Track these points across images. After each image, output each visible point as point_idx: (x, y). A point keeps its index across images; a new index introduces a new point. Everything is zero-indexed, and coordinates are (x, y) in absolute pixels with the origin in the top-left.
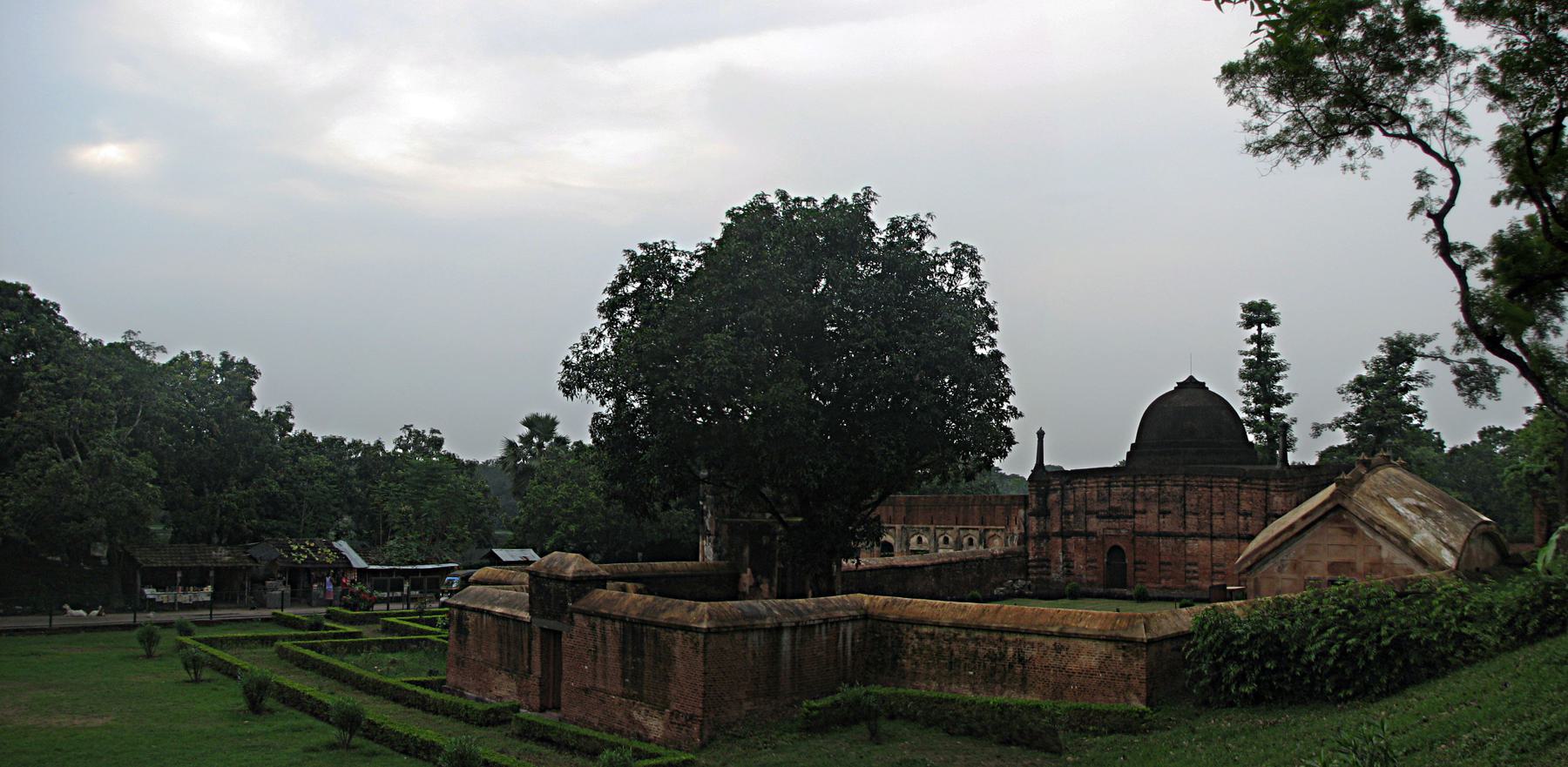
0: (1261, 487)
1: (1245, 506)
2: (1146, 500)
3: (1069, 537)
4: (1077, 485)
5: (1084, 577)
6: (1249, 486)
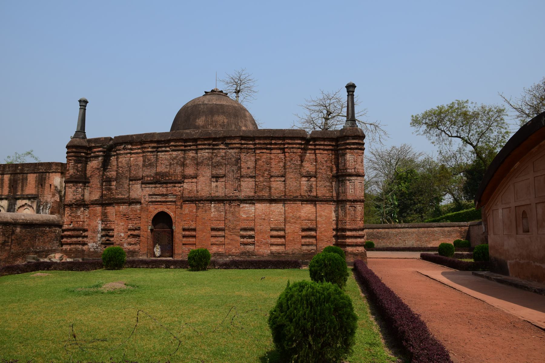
0: (326, 148)
1: (308, 167)
2: (197, 164)
3: (110, 204)
4: (122, 152)
5: (125, 246)
6: (313, 147)
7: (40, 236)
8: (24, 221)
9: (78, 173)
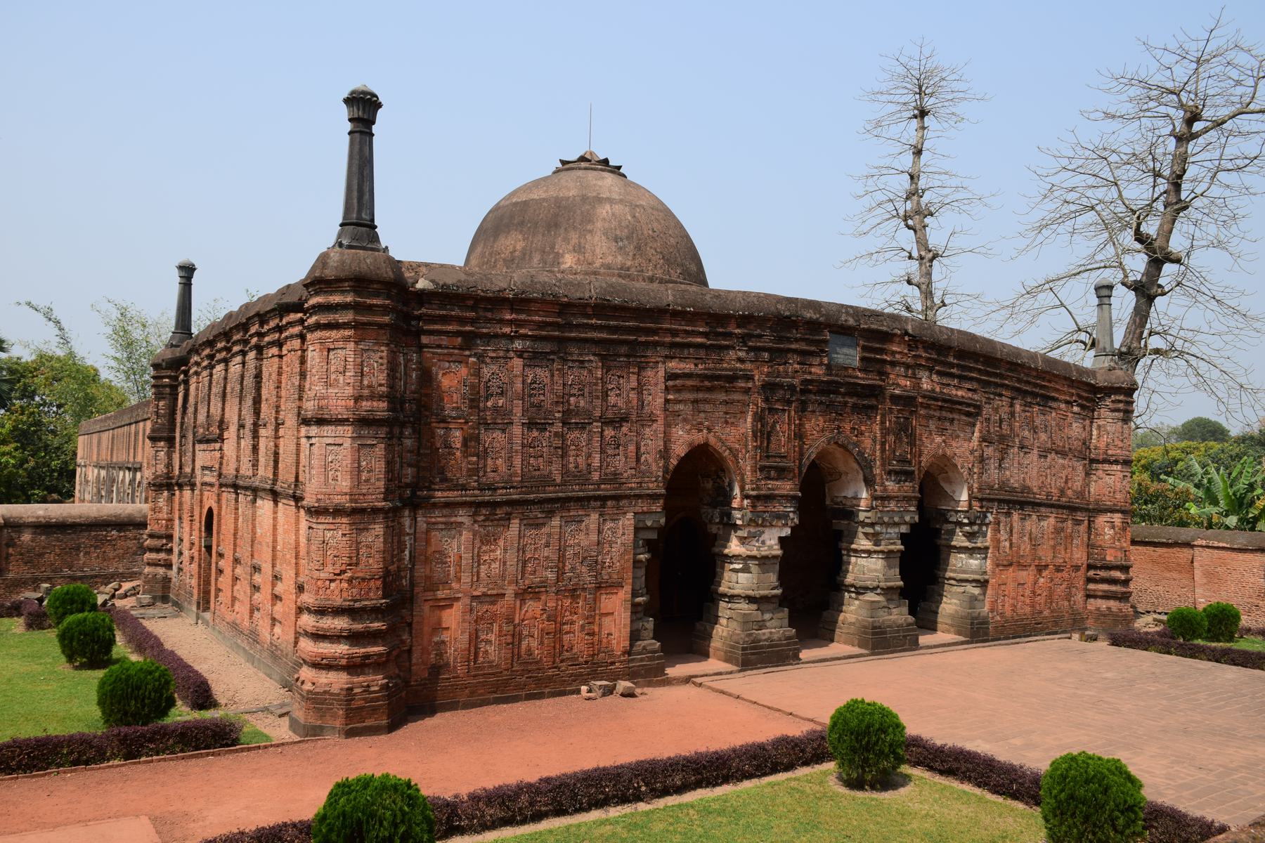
7: (92, 546)
8: (42, 520)
9: (159, 421)
